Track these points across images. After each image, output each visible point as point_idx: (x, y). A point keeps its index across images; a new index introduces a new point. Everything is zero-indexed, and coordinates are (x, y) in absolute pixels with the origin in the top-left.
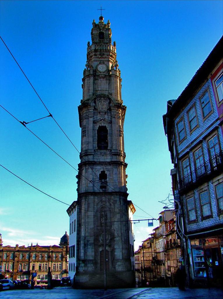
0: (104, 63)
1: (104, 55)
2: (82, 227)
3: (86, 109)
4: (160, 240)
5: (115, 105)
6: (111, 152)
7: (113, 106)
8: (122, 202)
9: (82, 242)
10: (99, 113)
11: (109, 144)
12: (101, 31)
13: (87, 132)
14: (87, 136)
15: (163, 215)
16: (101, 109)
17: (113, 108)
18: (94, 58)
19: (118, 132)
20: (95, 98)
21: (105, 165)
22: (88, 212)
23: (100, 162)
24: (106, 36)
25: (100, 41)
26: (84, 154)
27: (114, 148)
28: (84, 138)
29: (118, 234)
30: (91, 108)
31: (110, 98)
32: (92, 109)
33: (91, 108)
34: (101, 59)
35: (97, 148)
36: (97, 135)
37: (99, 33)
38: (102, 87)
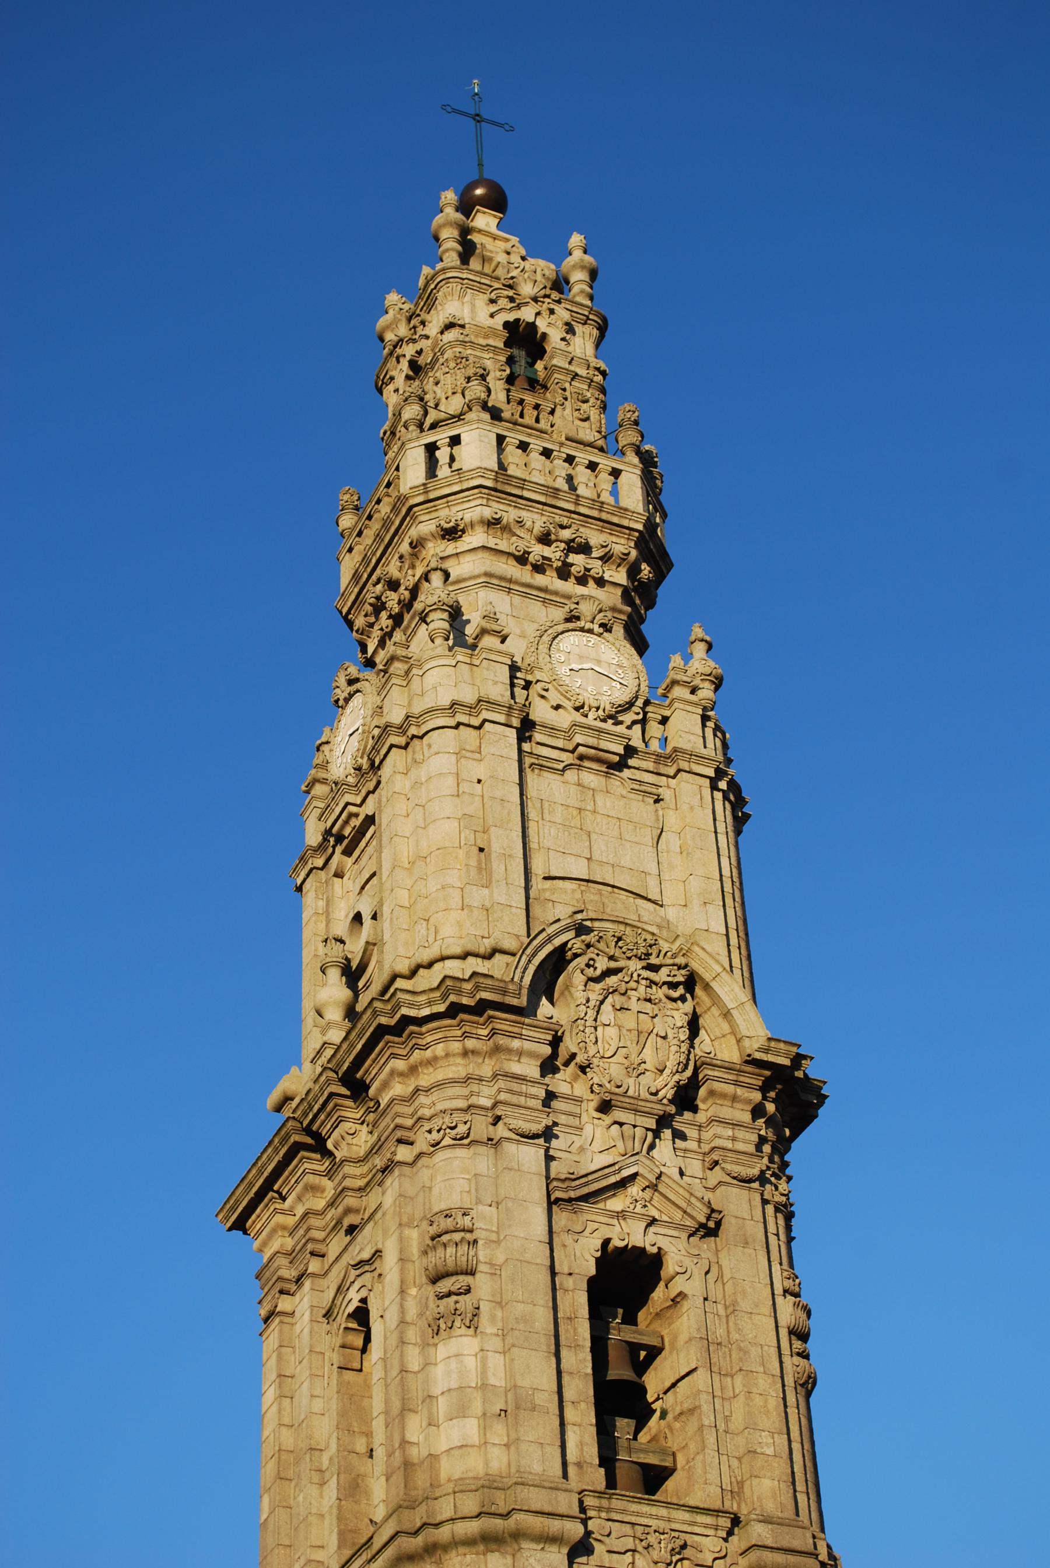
3: (470, 1044)
7: (729, 1068)
12: (527, 314)
16: (615, 1070)
17: (730, 1089)
18: (484, 547)
20: (563, 948)
27: (770, 1507)
28: (462, 1344)
30: (527, 1045)
31: (707, 976)
32: (532, 1055)
33: (527, 1045)
34: (540, 580)
35: (598, 1477)
36: (584, 1330)
37: (507, 325)
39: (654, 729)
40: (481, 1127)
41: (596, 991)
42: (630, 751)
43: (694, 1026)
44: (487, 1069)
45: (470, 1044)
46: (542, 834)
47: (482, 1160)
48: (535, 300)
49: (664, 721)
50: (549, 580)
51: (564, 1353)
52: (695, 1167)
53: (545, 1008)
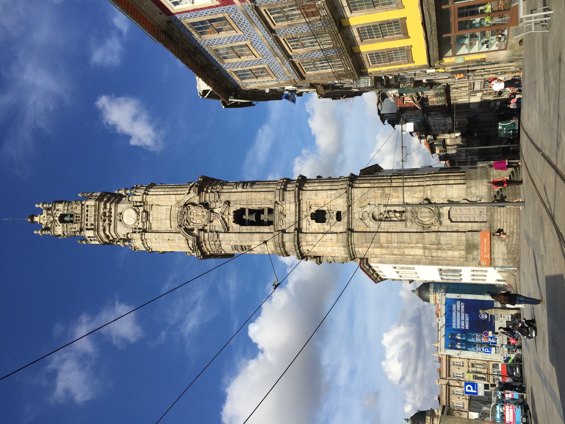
0: (121, 214)
1: (105, 214)
2: (406, 253)
3: (204, 245)
4: (431, 123)
5: (198, 195)
6: (279, 202)
7: (200, 198)
8: (365, 185)
9: (434, 254)
10: (211, 222)
11: (266, 206)
12: (57, 219)
13: (244, 244)
14: (250, 244)
15: (386, 117)
16: (204, 220)
19: (244, 190)
21: (301, 212)
22: (381, 242)
23: (296, 221)
24: (68, 209)
25: (77, 221)
26: (282, 249)
29: (420, 191)
35: (272, 226)
36: (249, 227)
38: (164, 217)
39: (138, 204)
40: (217, 243)
41: (191, 224)
42: (144, 211)
43: (194, 204)
44: (207, 242)
45: (204, 245)
46: (163, 229)
47: (223, 244)
48: (53, 217)
49: (136, 202)
50: (112, 219)
51: (253, 231)
52: (218, 204)
53: (195, 232)
